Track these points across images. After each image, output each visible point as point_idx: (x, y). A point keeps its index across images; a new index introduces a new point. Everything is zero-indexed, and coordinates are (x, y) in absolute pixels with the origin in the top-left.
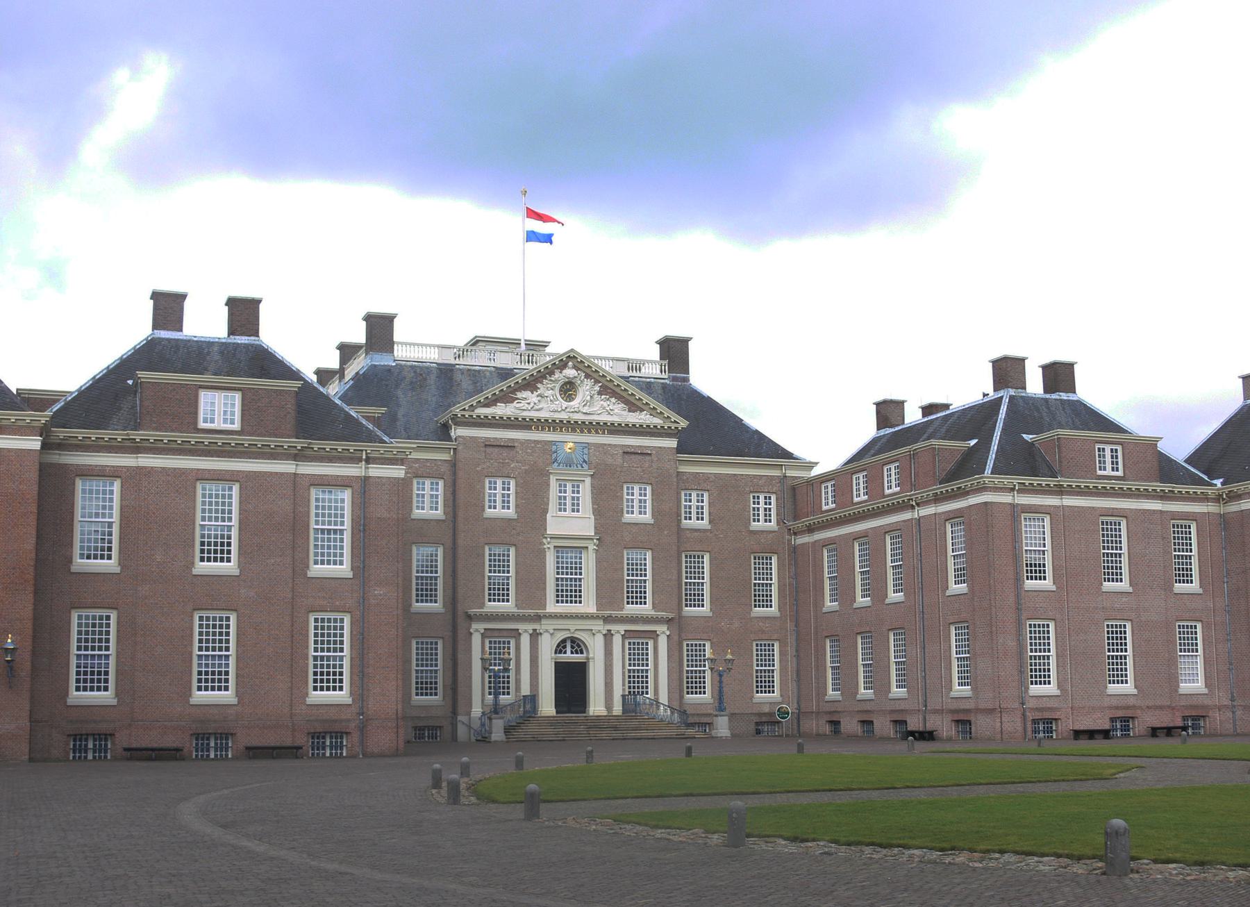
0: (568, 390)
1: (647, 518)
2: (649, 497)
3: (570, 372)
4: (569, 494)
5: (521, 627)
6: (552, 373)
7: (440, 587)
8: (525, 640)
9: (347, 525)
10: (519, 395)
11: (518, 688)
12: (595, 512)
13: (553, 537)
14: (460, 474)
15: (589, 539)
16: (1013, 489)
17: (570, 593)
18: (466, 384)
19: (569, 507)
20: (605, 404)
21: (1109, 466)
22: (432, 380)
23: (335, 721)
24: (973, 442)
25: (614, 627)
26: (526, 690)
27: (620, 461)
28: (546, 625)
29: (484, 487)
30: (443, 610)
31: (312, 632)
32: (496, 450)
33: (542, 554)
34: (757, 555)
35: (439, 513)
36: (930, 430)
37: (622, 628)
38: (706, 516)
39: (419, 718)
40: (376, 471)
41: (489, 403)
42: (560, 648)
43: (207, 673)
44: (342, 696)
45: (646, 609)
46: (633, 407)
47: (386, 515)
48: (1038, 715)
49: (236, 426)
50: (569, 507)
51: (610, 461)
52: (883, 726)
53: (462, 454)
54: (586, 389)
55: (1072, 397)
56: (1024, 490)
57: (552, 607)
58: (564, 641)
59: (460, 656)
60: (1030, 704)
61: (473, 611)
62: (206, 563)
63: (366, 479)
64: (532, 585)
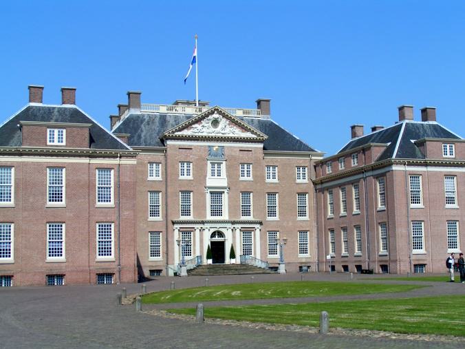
0: (215, 123)
1: (251, 178)
2: (251, 169)
3: (216, 116)
4: (216, 169)
5: (196, 226)
6: (208, 116)
7: (160, 210)
8: (198, 231)
9: (112, 185)
10: (193, 126)
11: (194, 253)
12: (229, 176)
14: (168, 161)
16: (405, 164)
17: (217, 211)
18: (172, 121)
20: (231, 129)
21: (448, 153)
22: (157, 120)
23: (107, 269)
24: (389, 144)
25: (236, 226)
26: (198, 254)
27: (238, 152)
30: (162, 220)
31: (98, 230)
33: (204, 195)
34: (101, 224)
35: (160, 178)
36: (373, 138)
37: (240, 226)
38: (277, 177)
39: (153, 266)
40: (125, 161)
41: (180, 130)
42: (213, 235)
43: (53, 249)
44: (112, 258)
45: (250, 218)
46: (245, 129)
47: (128, 180)
48: (417, 263)
51: (233, 154)
52: (352, 268)
55: (435, 123)
56: (410, 164)
58: (214, 232)
59: (169, 239)
60: (413, 258)
62: (51, 202)
64: (200, 207)
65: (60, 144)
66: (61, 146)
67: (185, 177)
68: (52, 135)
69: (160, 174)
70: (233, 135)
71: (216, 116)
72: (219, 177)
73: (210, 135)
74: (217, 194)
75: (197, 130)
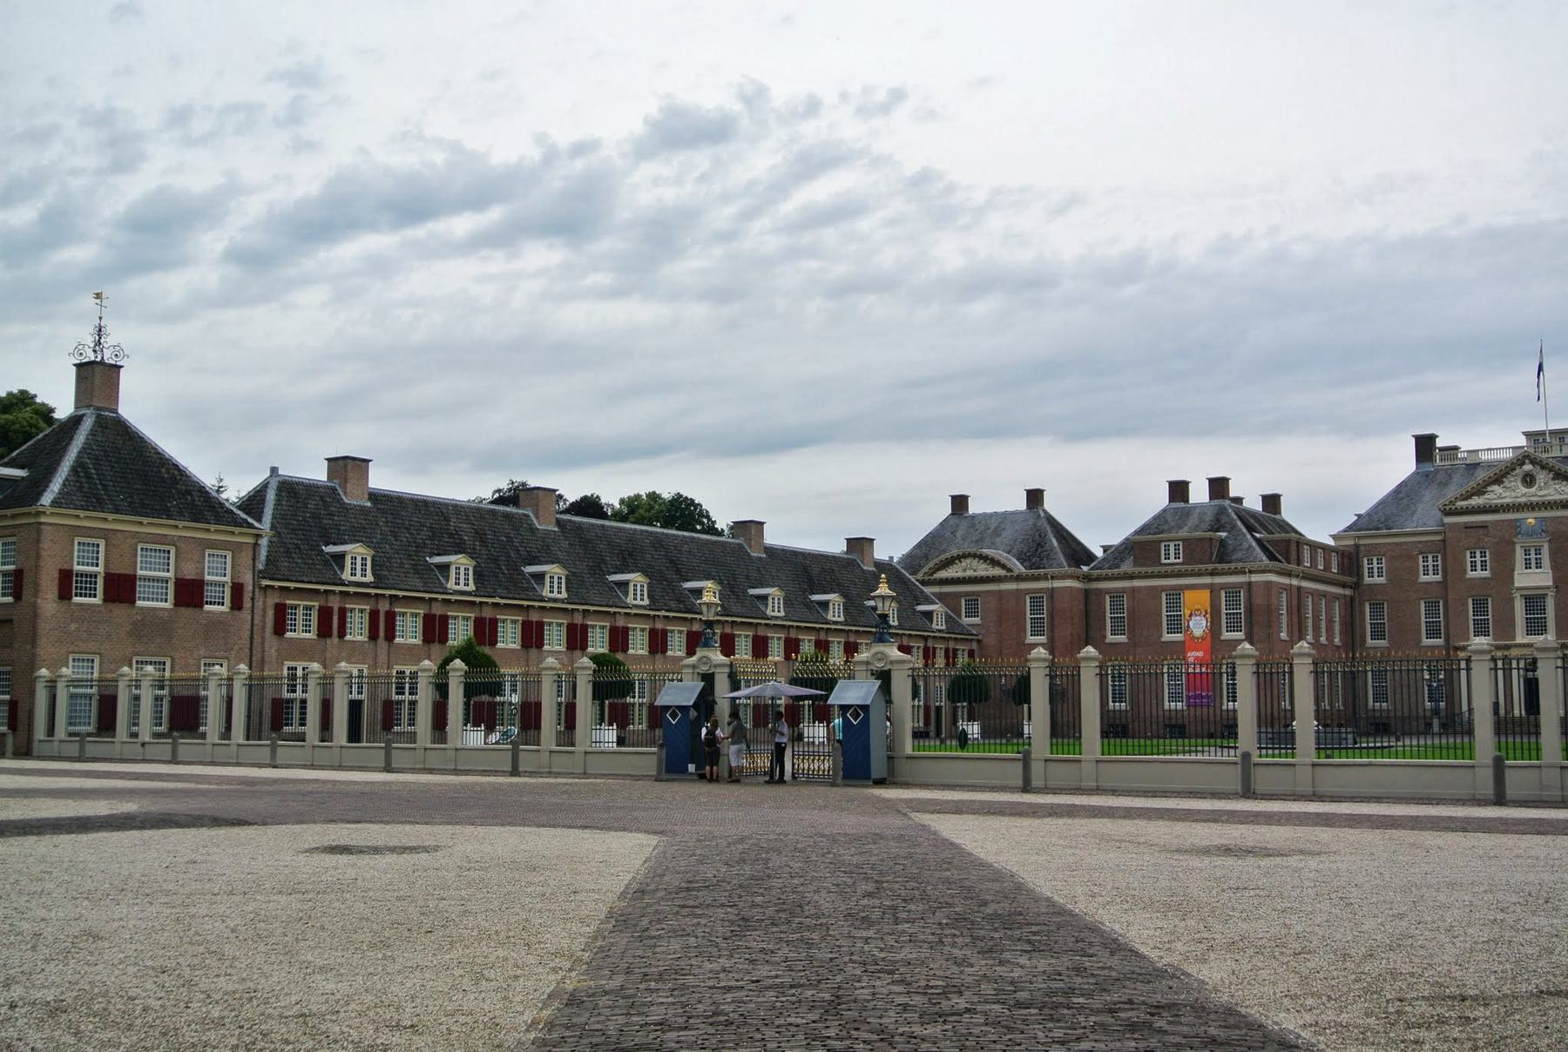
3: (1528, 467)
4: (1533, 556)
6: (1515, 469)
10: (1489, 489)
13: (1519, 589)
15: (1548, 588)
19: (1533, 565)
28: (1514, 652)
29: (1465, 558)
32: (1474, 530)
33: (1512, 600)
35: (1438, 578)
40: (1255, 578)
49: (1181, 560)
50: (1533, 565)
53: (1449, 535)
54: (1542, 477)
57: (1521, 638)
61: (1457, 645)
63: (1250, 584)
64: (1507, 627)
65: (1177, 561)
66: (1177, 564)
67: (1479, 573)
68: (1167, 548)
69: (1440, 572)
70: (1562, 497)
71: (1528, 467)
72: (1539, 570)
73: (1518, 500)
74: (1534, 601)
75: (1498, 495)
